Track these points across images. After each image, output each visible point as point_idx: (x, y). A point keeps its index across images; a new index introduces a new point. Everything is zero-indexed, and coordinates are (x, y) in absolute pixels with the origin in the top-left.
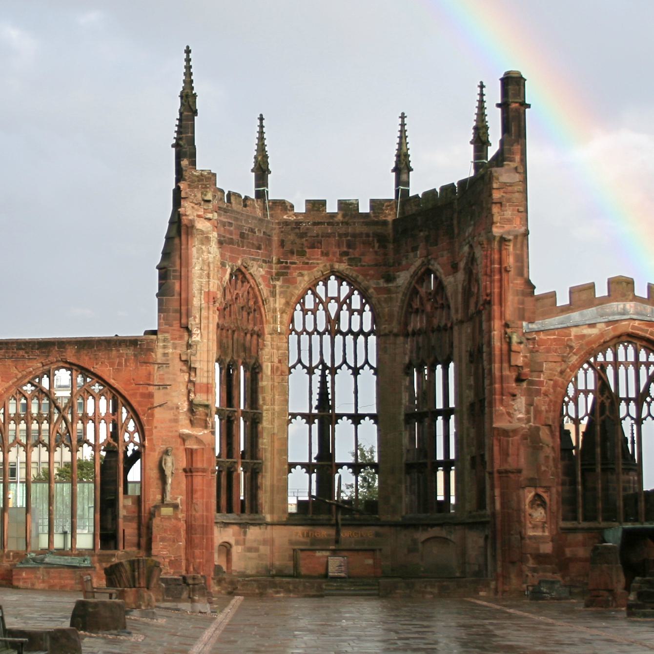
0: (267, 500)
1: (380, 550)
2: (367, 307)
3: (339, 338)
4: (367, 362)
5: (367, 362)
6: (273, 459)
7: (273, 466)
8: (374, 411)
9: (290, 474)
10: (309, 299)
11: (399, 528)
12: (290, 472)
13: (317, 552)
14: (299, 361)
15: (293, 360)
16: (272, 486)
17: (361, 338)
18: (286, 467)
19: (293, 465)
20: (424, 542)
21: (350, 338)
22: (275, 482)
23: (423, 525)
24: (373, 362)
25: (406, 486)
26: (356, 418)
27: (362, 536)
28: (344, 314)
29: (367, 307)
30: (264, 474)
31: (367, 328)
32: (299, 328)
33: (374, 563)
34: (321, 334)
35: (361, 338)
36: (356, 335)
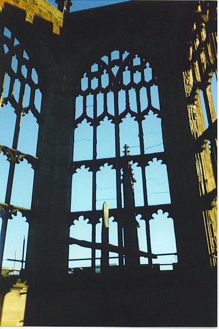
2: (148, 64)
3: (122, 93)
4: (150, 107)
5: (150, 107)
8: (161, 149)
10: (95, 68)
14: (84, 115)
15: (78, 113)
17: (143, 91)
19: (77, 215)
21: (132, 92)
24: (156, 104)
26: (143, 160)
28: (126, 75)
29: (148, 64)
31: (148, 77)
32: (84, 87)
34: (105, 92)
35: (143, 91)
36: (138, 88)
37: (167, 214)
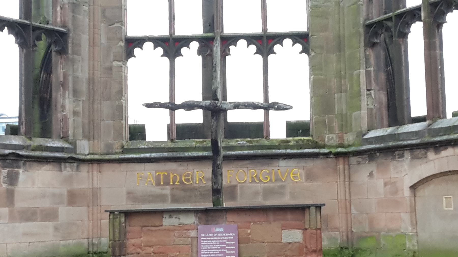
0: (80, 109)
1: (318, 207)
6: (94, 27)
7: (93, 43)
9: (131, 60)
11: (354, 160)
12: (130, 54)
13: (166, 216)
16: (91, 81)
18: (122, 44)
20: (414, 188)
22: (98, 74)
23: (412, 147)
25: (368, 73)
27: (278, 180)
30: (71, 56)
33: (304, 239)
37: (299, 47)
